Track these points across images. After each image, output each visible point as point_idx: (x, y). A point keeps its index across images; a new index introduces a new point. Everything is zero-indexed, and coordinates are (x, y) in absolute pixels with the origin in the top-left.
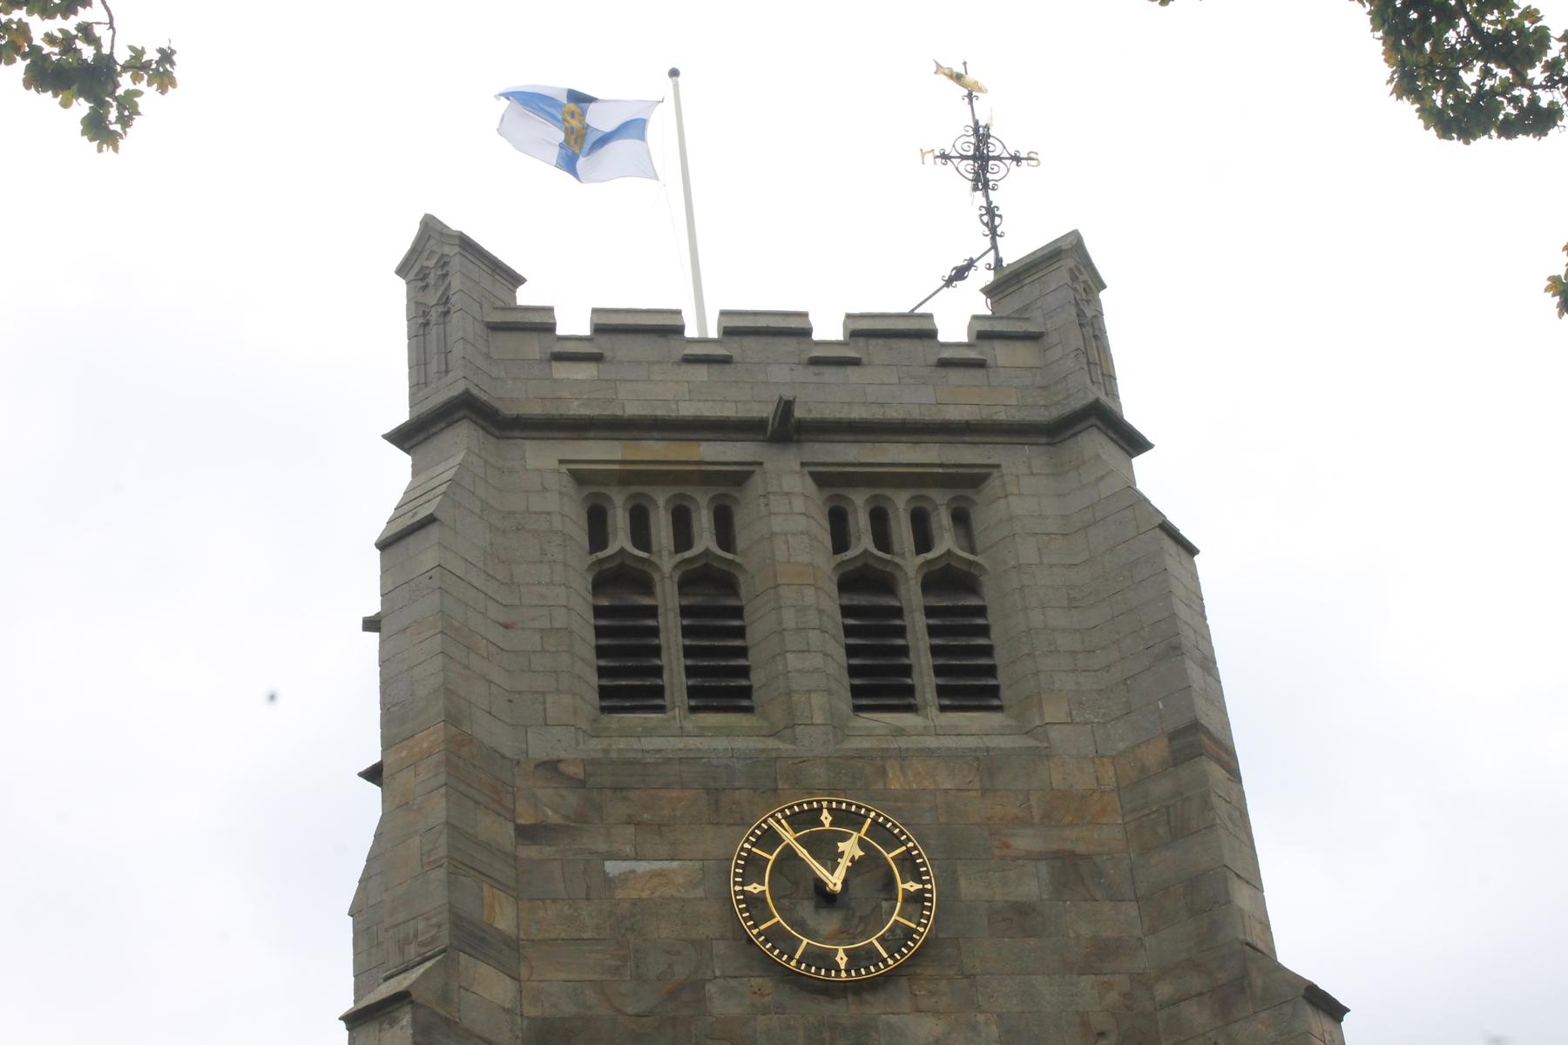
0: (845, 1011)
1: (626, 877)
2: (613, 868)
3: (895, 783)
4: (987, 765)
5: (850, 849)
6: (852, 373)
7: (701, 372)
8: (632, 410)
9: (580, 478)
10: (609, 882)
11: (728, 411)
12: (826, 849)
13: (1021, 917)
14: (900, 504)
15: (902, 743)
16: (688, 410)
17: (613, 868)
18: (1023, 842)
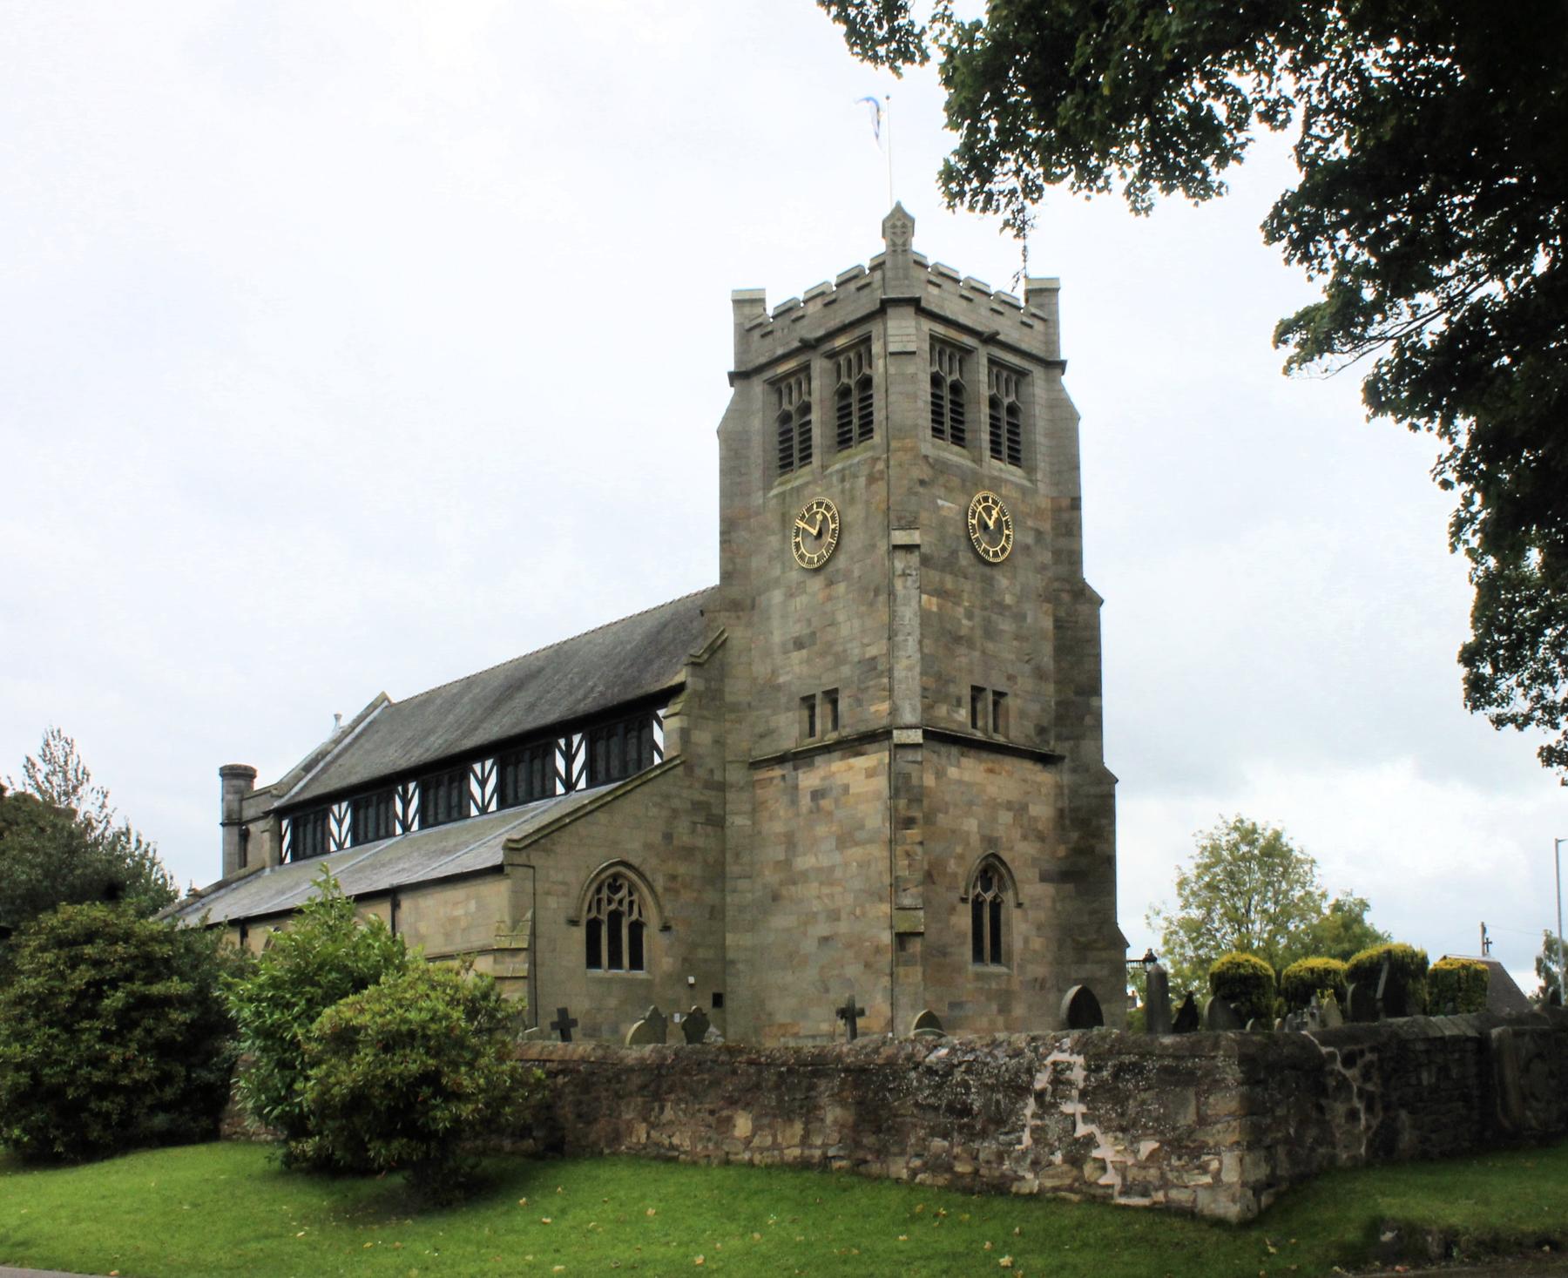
0: (987, 570)
1: (943, 506)
2: (940, 502)
3: (1004, 491)
4: (1024, 491)
5: (994, 513)
6: (1000, 317)
7: (964, 303)
8: (949, 314)
9: (932, 337)
10: (939, 508)
11: (969, 323)
12: (988, 510)
13: (1027, 548)
14: (1005, 374)
15: (1004, 476)
16: (962, 320)
17: (940, 502)
18: (1030, 523)
